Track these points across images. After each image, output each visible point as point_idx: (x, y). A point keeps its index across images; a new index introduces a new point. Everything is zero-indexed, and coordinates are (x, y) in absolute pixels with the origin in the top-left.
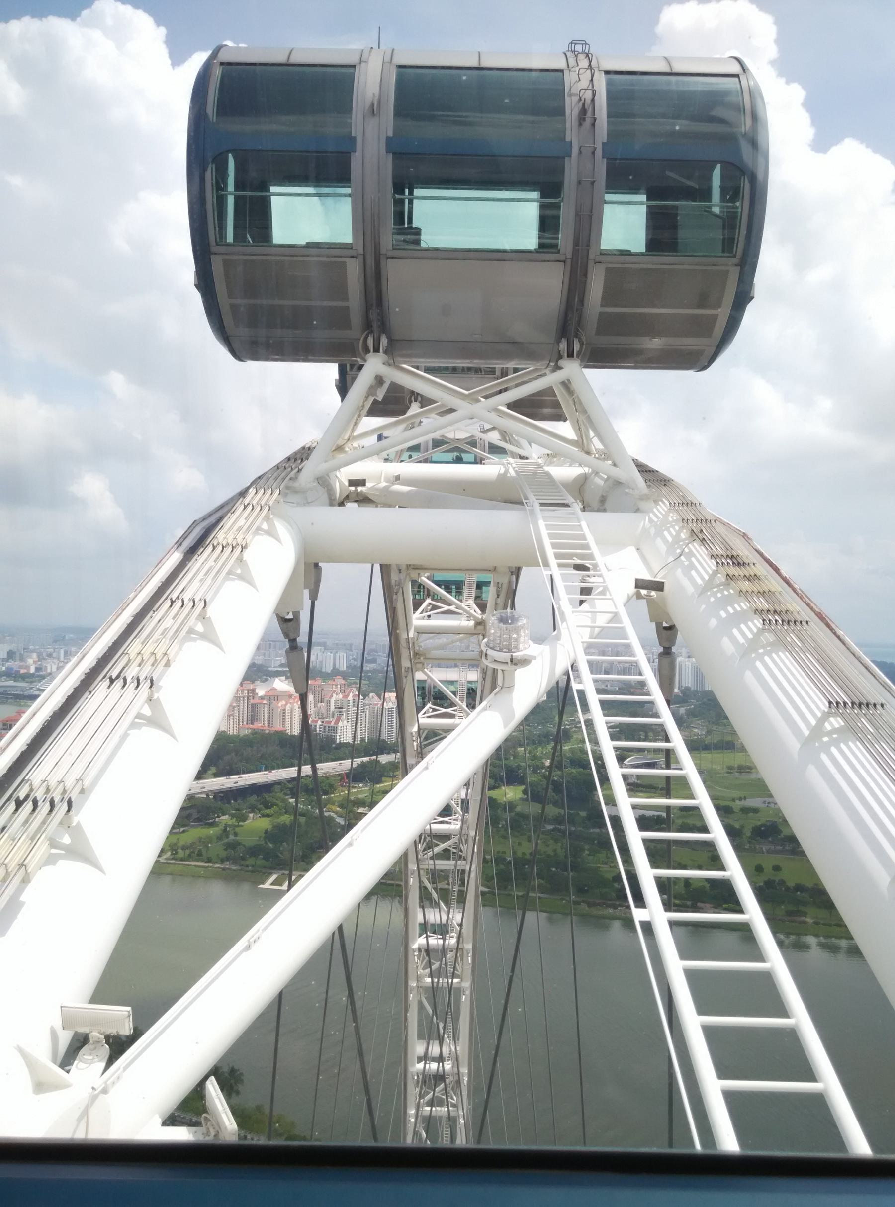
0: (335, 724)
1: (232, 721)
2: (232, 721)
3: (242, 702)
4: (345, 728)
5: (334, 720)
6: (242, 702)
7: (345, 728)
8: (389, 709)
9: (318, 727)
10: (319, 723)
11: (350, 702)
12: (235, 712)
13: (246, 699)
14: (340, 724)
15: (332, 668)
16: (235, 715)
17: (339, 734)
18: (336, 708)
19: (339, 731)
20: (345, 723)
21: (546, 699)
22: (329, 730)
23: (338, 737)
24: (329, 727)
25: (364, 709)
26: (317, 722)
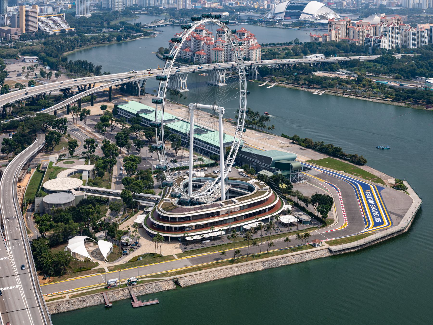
0: (380, 38)
1: (337, 36)
2: (337, 36)
3: (343, 27)
4: (385, 41)
6: (343, 27)
7: (385, 41)
9: (372, 40)
10: (373, 38)
13: (345, 25)
14: (382, 39)
15: (427, 7)
17: (382, 43)
18: (383, 31)
19: (382, 42)
23: (381, 45)
26: (372, 37)
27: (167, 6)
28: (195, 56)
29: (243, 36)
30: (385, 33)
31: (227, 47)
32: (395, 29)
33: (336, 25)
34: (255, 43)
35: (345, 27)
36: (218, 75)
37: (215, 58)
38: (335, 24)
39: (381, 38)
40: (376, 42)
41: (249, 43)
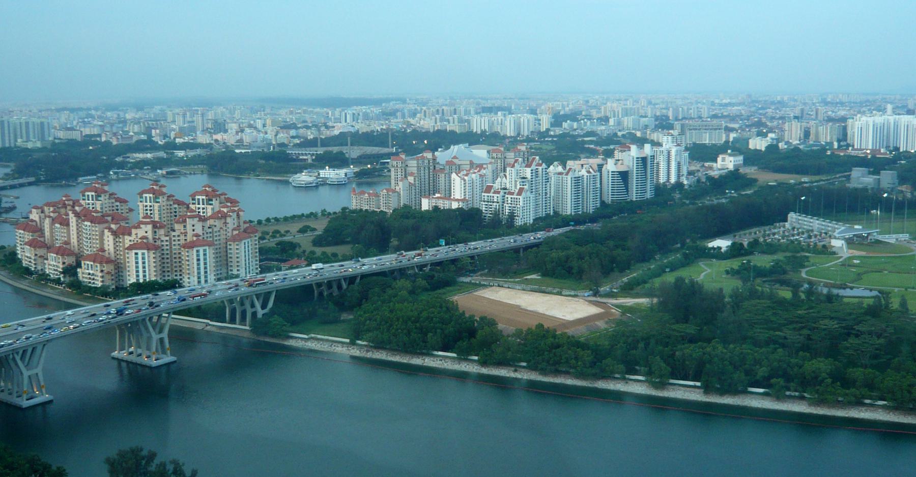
3: (422, 172)
4: (528, 199)
5: (517, 191)
7: (528, 199)
8: (575, 178)
11: (534, 171)
12: (417, 182)
16: (417, 185)
20: (528, 193)
21: (742, 162)
22: (511, 201)
24: (511, 198)
25: (548, 179)
27: (39, 145)
28: (81, 267)
29: (208, 206)
30: (523, 182)
31: (167, 238)
32: (540, 172)
33: (408, 169)
34: (242, 224)
35: (427, 171)
36: (145, 335)
37: (138, 276)
38: (407, 166)
39: (519, 193)
40: (509, 202)
41: (225, 223)
